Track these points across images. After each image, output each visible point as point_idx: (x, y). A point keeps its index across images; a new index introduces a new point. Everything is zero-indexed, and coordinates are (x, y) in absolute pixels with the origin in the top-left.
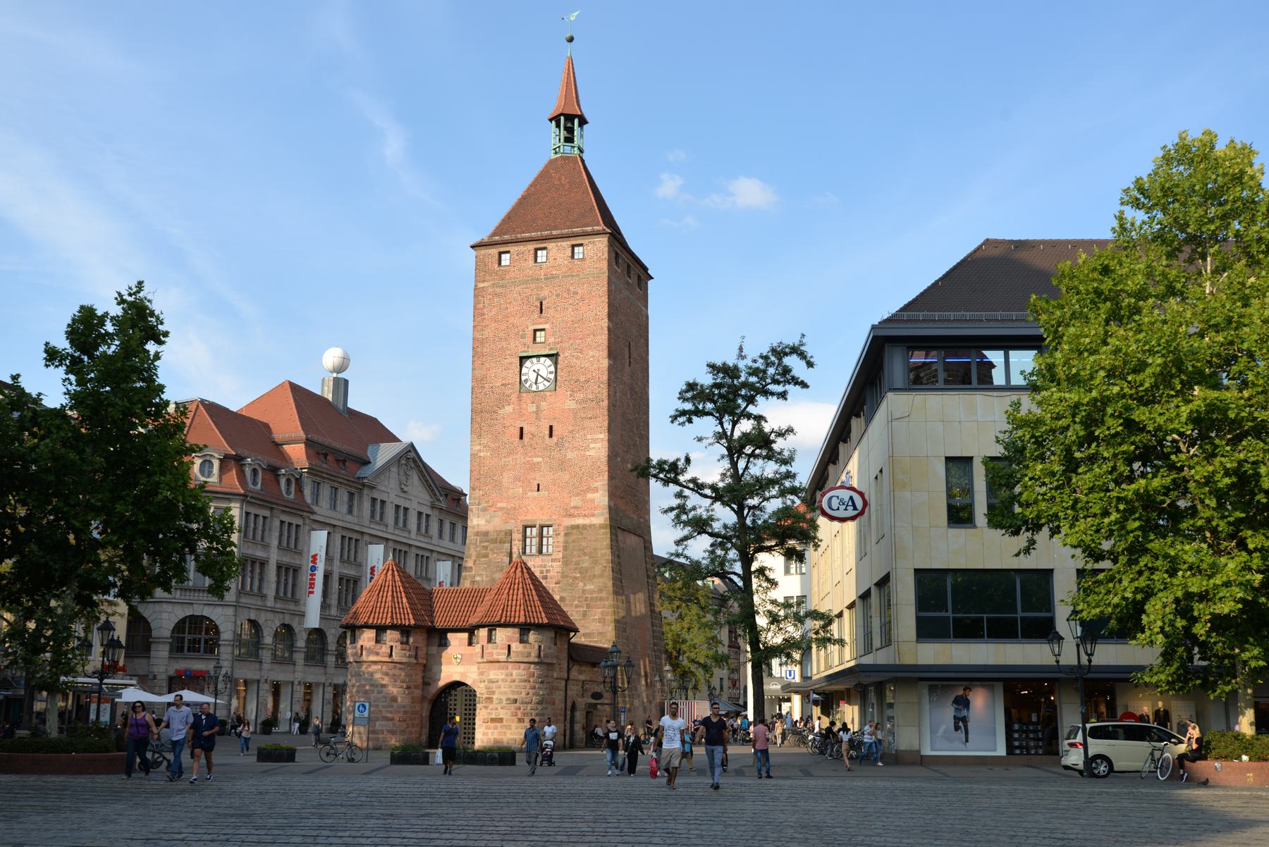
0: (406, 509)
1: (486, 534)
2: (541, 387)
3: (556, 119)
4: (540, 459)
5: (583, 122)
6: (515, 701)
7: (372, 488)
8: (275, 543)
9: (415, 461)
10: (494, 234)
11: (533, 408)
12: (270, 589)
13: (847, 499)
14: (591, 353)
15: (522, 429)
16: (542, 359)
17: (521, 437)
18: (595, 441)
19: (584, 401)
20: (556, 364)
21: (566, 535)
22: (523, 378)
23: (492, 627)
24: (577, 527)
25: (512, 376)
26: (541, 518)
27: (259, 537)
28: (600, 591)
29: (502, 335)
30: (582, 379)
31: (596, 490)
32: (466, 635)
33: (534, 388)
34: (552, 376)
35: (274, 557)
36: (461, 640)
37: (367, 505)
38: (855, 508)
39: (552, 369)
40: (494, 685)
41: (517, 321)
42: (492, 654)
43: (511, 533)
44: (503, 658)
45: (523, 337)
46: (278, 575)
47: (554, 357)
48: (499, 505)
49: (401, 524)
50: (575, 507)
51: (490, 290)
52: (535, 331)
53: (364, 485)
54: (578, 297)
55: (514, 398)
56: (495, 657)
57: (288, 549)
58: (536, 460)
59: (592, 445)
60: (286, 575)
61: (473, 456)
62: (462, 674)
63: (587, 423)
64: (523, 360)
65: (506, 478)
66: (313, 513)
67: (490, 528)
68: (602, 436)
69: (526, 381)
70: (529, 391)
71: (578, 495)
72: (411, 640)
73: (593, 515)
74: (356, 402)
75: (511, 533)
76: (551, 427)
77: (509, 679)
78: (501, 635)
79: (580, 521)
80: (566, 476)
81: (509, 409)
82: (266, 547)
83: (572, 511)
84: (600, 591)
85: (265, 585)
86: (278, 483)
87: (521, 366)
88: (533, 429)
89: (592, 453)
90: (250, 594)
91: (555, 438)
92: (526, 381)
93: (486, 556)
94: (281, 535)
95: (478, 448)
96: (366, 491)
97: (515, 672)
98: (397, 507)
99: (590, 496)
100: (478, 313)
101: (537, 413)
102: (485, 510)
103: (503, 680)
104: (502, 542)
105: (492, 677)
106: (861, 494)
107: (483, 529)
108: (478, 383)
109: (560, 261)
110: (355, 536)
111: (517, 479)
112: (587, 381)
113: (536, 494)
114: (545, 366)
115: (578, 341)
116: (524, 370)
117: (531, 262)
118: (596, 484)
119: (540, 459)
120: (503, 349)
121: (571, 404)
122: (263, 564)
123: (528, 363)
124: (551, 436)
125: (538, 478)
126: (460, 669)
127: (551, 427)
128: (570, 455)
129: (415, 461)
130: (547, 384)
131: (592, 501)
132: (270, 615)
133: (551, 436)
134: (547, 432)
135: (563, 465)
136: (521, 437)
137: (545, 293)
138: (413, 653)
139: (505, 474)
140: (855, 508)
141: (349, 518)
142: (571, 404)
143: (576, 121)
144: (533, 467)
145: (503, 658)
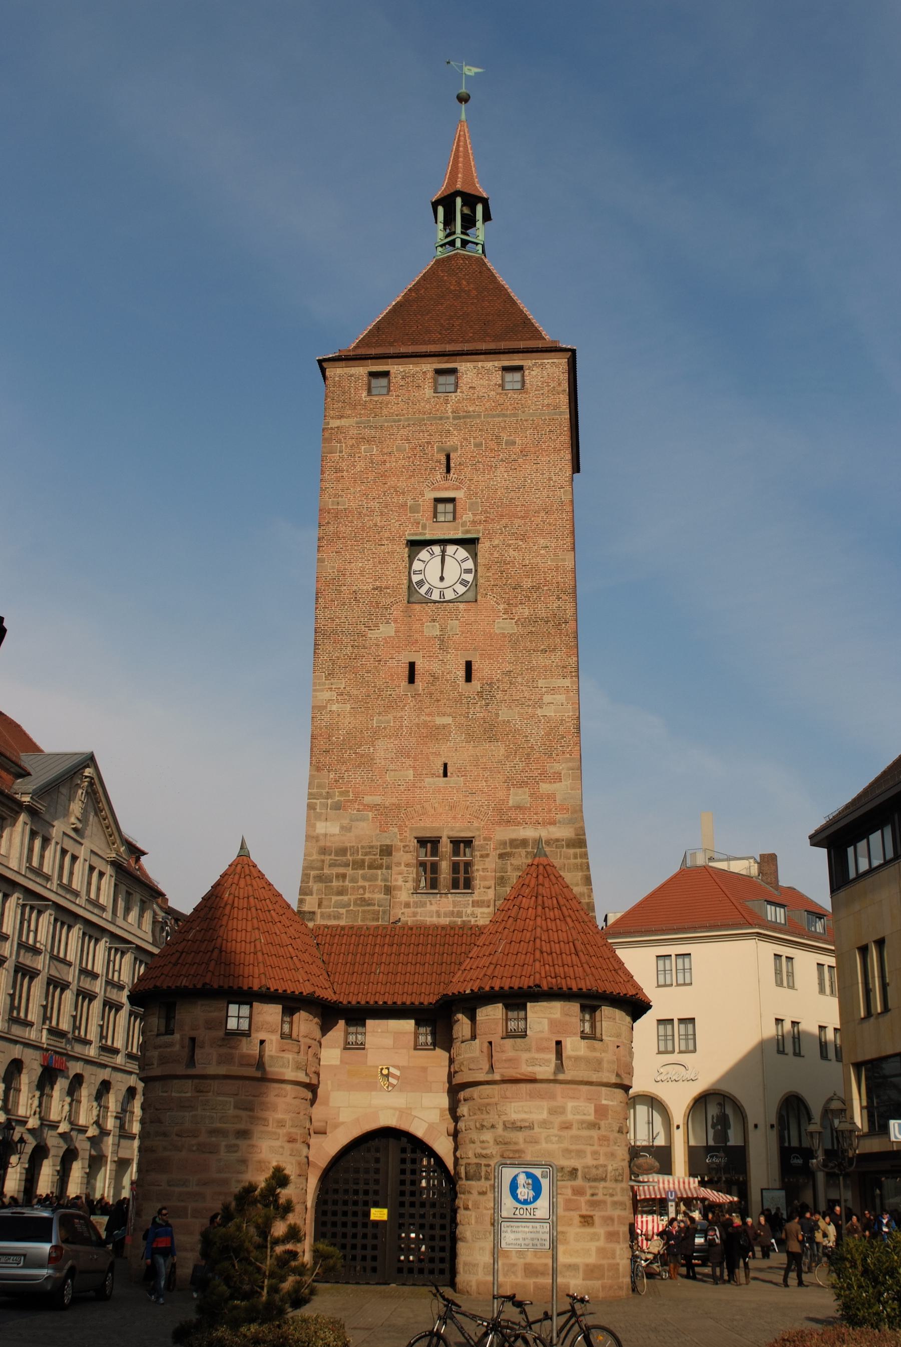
1: (343, 851)
2: (449, 595)
3: (447, 202)
4: (448, 720)
5: (487, 217)
6: (573, 1173)
10: (363, 343)
14: (542, 542)
15: (412, 666)
16: (451, 549)
17: (411, 679)
18: (553, 690)
19: (533, 620)
20: (475, 556)
21: (501, 856)
22: (415, 578)
23: (516, 999)
24: (524, 843)
25: (394, 576)
26: (448, 827)
29: (374, 505)
30: (527, 583)
31: (557, 777)
33: (435, 596)
34: (469, 577)
36: (397, 1035)
39: (470, 564)
40: (520, 1137)
41: (402, 485)
42: (513, 1061)
43: (387, 851)
44: (546, 1070)
45: (414, 509)
47: (469, 543)
48: (368, 799)
50: (518, 808)
51: (353, 432)
52: (438, 500)
54: (517, 449)
55: (397, 612)
56: (526, 1069)
58: (439, 721)
59: (547, 698)
61: (318, 709)
62: (403, 1112)
63: (540, 660)
64: (416, 545)
65: (383, 750)
67: (349, 840)
69: (421, 583)
70: (427, 601)
71: (522, 784)
73: (553, 823)
75: (387, 851)
76: (469, 665)
77: (557, 1120)
78: (542, 1017)
79: (529, 833)
80: (499, 750)
81: (387, 630)
83: (512, 814)
87: (411, 559)
88: (435, 667)
89: (549, 711)
91: (476, 684)
92: (421, 583)
93: (341, 892)
95: (327, 695)
97: (570, 1105)
98: (64, 852)
99: (545, 787)
102: (337, 807)
103: (544, 1124)
105: (514, 1116)
109: (481, 391)
111: (403, 753)
112: (536, 588)
115: (517, 522)
116: (417, 565)
117: (428, 392)
118: (558, 767)
119: (448, 720)
121: (504, 626)
123: (424, 554)
124: (468, 678)
126: (398, 1100)
127: (469, 665)
128: (505, 714)
130: (461, 589)
131: (551, 797)
133: (468, 678)
134: (462, 673)
135: (491, 731)
136: (411, 679)
137: (454, 440)
139: (381, 744)
142: (504, 626)
143: (479, 208)
144: (436, 734)
145: (546, 1070)
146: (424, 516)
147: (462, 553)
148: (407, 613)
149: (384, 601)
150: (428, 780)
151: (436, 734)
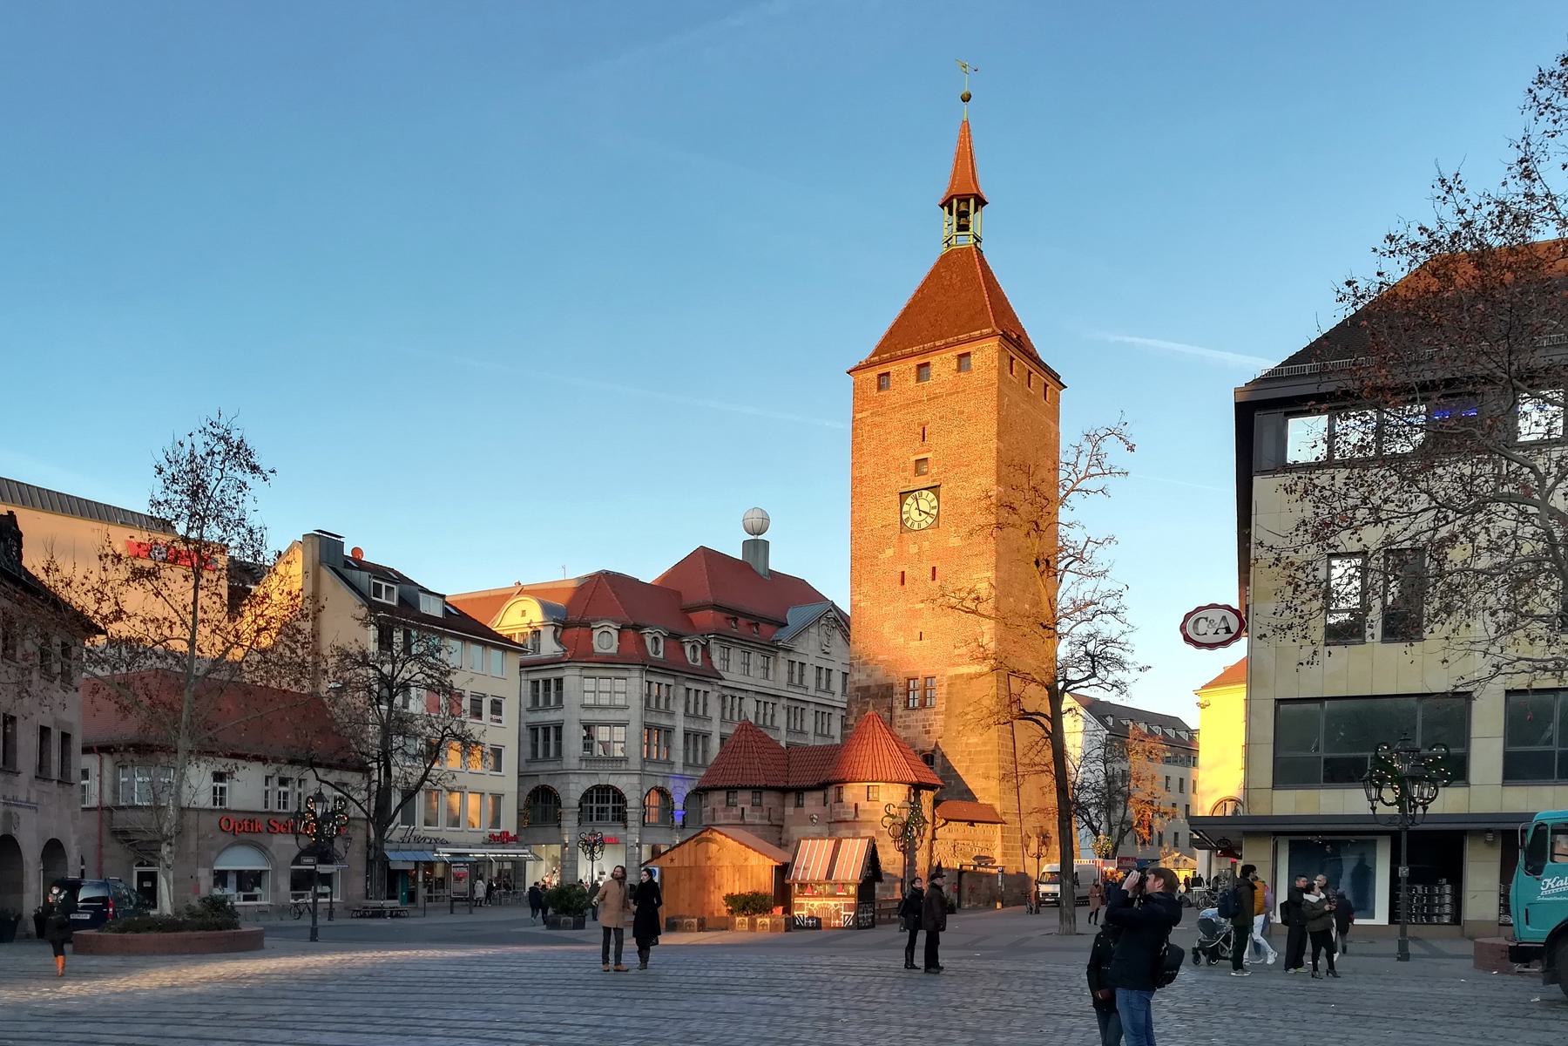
0: (829, 671)
2: (924, 525)
7: (789, 651)
8: (681, 710)
9: (836, 620)
11: (914, 549)
12: (678, 756)
13: (1218, 620)
20: (938, 498)
27: (662, 706)
28: (984, 744)
29: (882, 471)
32: (820, 795)
34: (934, 512)
35: (680, 724)
37: (783, 668)
38: (1228, 630)
39: (935, 503)
41: (897, 453)
46: (686, 742)
47: (934, 489)
49: (823, 687)
53: (778, 648)
55: (895, 541)
57: (696, 716)
60: (696, 744)
64: (903, 496)
66: (722, 679)
68: (989, 574)
72: (765, 800)
74: (779, 562)
81: (890, 552)
82: (671, 714)
84: (984, 744)
85: (672, 753)
86: (683, 650)
88: (916, 573)
90: (658, 762)
91: (938, 582)
94: (687, 702)
96: (781, 654)
100: (857, 448)
101: (918, 554)
104: (884, 696)
106: (1237, 613)
107: (865, 684)
108: (857, 526)
110: (771, 700)
111: (899, 628)
113: (918, 643)
114: (927, 501)
116: (906, 508)
120: (883, 487)
121: (954, 542)
122: (669, 731)
123: (910, 500)
125: (920, 625)
129: (836, 620)
130: (930, 520)
132: (678, 782)
138: (766, 813)
139: (887, 625)
140: (1228, 630)
141: (765, 683)
144: (915, 614)
146: (909, 474)
147: (931, 496)
148: (901, 540)
149: (888, 534)
150: (912, 644)
151: (915, 614)
